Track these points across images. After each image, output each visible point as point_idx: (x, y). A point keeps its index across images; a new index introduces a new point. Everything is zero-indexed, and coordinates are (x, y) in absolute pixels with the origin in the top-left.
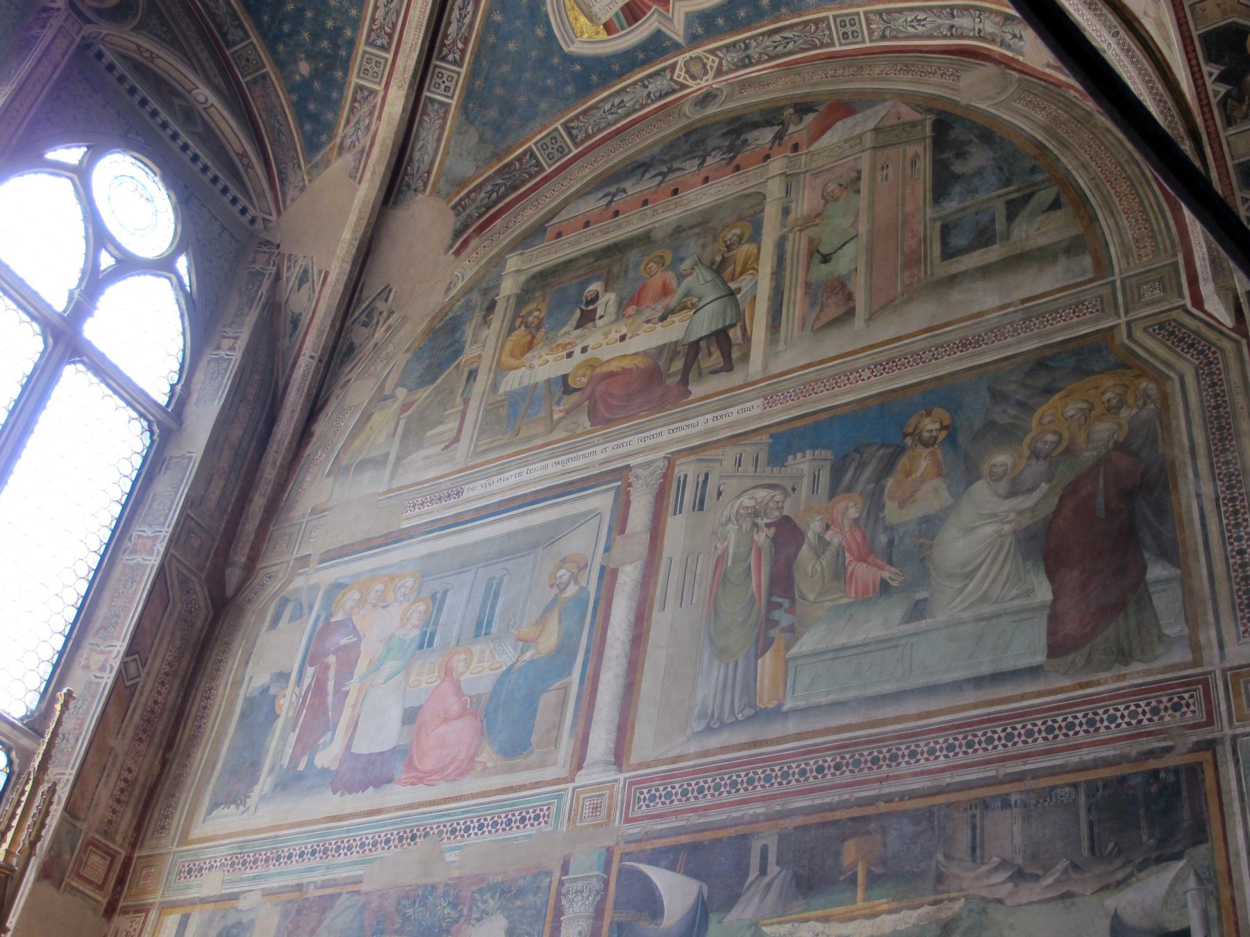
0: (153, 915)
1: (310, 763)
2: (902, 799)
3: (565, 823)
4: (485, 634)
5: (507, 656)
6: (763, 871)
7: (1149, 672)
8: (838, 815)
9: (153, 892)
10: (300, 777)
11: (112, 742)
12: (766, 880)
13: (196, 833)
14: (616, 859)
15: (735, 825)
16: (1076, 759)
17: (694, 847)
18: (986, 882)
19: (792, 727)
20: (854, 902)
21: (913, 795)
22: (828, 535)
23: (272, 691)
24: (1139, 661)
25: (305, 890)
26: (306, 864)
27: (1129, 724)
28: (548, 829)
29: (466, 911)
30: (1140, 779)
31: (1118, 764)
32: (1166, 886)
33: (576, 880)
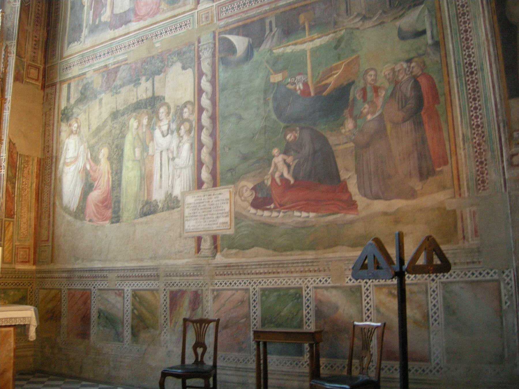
0: (58, 86)
1: (100, 21)
3: (196, 25)
6: (271, 30)
9: (56, 78)
11: (26, 28)
12: (273, 32)
13: (65, 54)
14: (217, 35)
15: (259, 15)
17: (245, 26)
20: (305, 36)
26: (106, 58)
28: (190, 28)
32: (417, 15)
33: (203, 45)
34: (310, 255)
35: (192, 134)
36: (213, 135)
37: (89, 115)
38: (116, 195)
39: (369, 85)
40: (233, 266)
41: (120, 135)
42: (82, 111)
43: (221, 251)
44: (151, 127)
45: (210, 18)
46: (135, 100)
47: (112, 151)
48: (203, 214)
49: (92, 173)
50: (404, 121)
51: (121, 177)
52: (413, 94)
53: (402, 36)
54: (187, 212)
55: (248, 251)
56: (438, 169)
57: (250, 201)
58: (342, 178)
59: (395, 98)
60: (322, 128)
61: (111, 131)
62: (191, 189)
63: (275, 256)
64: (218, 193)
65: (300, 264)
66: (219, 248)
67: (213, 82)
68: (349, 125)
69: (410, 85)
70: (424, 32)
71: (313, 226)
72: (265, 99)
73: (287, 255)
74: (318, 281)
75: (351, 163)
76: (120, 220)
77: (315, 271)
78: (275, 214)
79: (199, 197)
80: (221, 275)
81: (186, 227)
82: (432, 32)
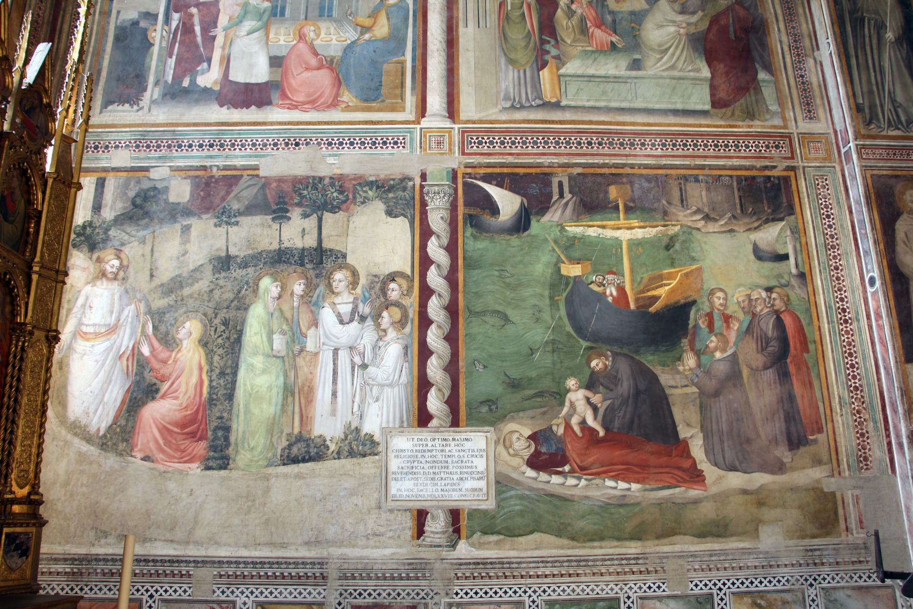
1: (193, 82)
2: (639, 168)
4: (328, 16)
5: (351, 35)
6: (561, 195)
7: (764, 127)
8: (603, 171)
10: (186, 92)
12: (564, 201)
14: (460, 176)
16: (730, 163)
18: (690, 219)
19: (568, 116)
21: (646, 167)
22: (574, 7)
23: (143, 24)
24: (759, 120)
25: (209, 170)
26: (206, 153)
27: (755, 150)
29: (351, 196)
30: (762, 179)
31: (752, 170)
34: (633, 548)
35: (408, 329)
36: (451, 338)
37: (152, 250)
38: (218, 414)
39: (716, 311)
40: (491, 563)
41: (236, 302)
42: (133, 239)
43: (467, 538)
44: (311, 302)
45: (446, 145)
46: (275, 246)
47: (213, 329)
48: (431, 471)
49: (155, 364)
50: (766, 368)
51: (234, 382)
52: (775, 334)
53: (759, 254)
54: (394, 465)
55: (520, 539)
56: (811, 437)
57: (526, 458)
58: (682, 435)
59: (753, 337)
60: (650, 360)
61: (212, 291)
62: (405, 424)
63: (573, 548)
64: (462, 437)
65: (616, 562)
66: (464, 532)
67: (451, 248)
68: (690, 361)
69: (772, 321)
70: (785, 257)
71: (638, 504)
72: (551, 298)
73: (594, 547)
74: (645, 588)
75: (694, 415)
76: (228, 464)
77: (641, 572)
78: (571, 481)
79: (421, 440)
80: (466, 578)
81: (393, 490)
82: (796, 259)
